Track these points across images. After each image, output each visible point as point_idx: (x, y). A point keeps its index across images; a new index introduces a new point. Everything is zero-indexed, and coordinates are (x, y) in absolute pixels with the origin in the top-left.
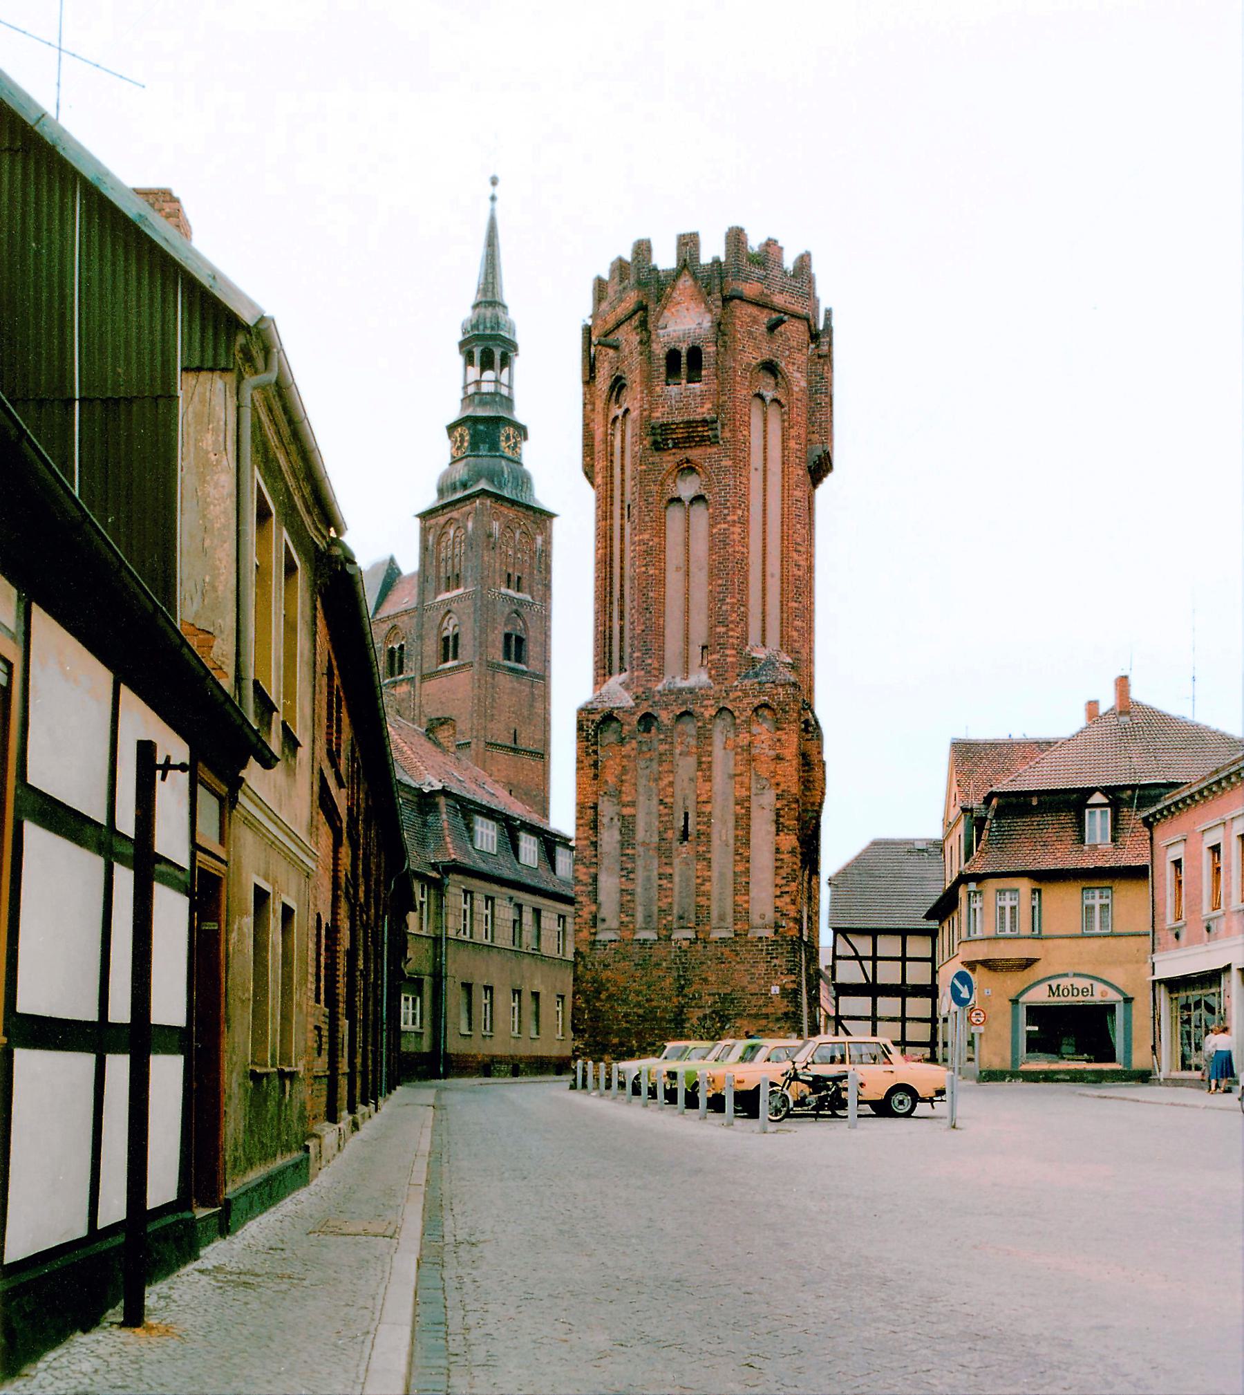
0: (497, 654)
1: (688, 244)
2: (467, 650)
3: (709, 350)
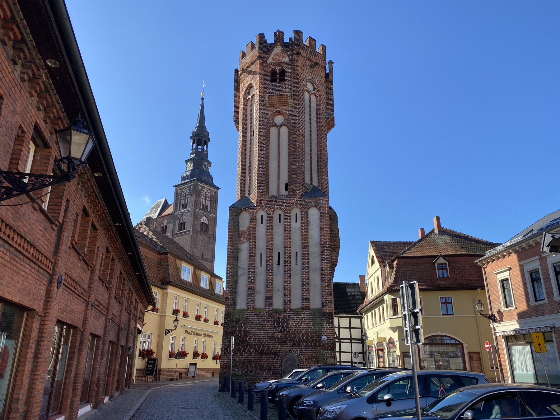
0: (199, 229)
1: (279, 36)
2: (189, 227)
3: (288, 70)
